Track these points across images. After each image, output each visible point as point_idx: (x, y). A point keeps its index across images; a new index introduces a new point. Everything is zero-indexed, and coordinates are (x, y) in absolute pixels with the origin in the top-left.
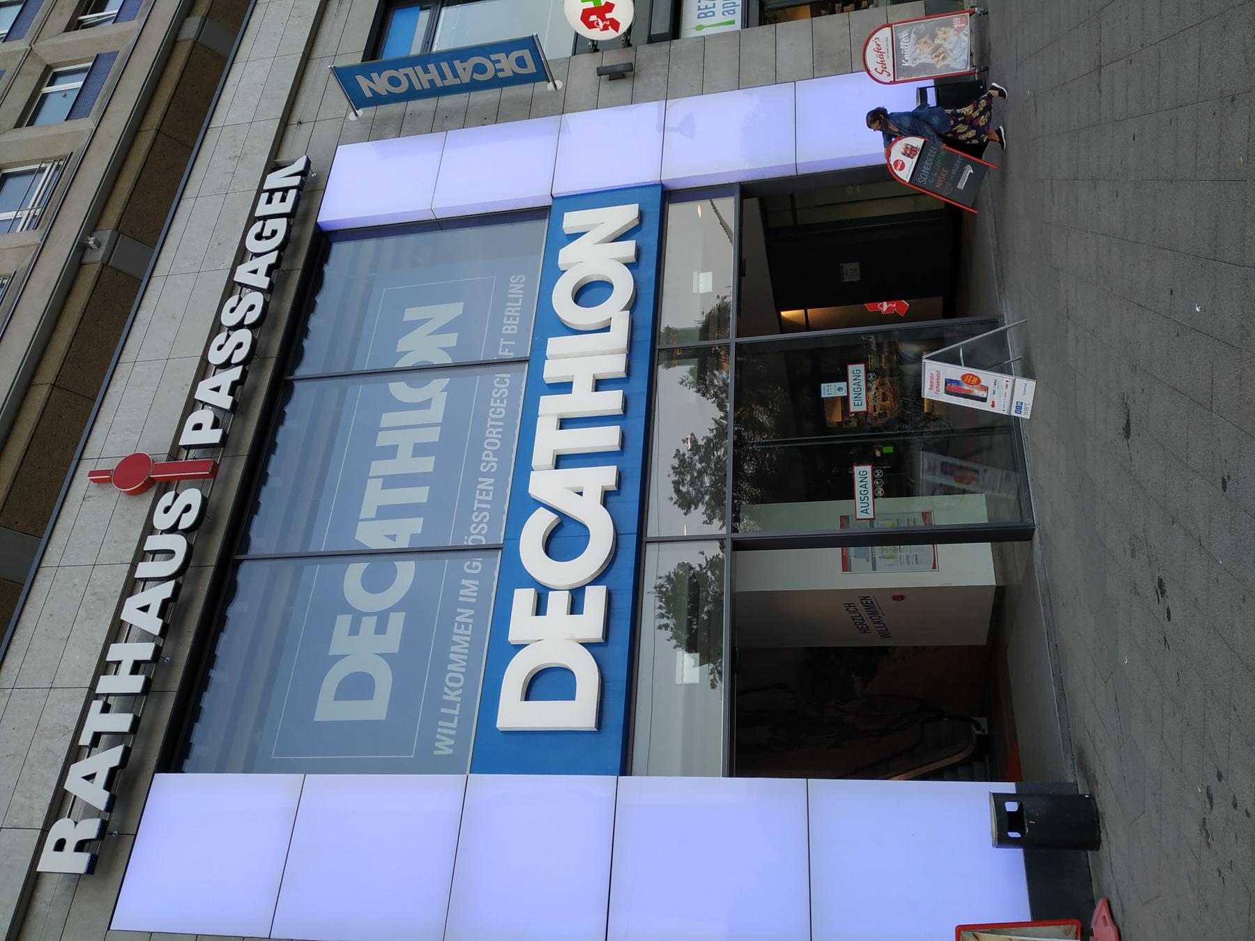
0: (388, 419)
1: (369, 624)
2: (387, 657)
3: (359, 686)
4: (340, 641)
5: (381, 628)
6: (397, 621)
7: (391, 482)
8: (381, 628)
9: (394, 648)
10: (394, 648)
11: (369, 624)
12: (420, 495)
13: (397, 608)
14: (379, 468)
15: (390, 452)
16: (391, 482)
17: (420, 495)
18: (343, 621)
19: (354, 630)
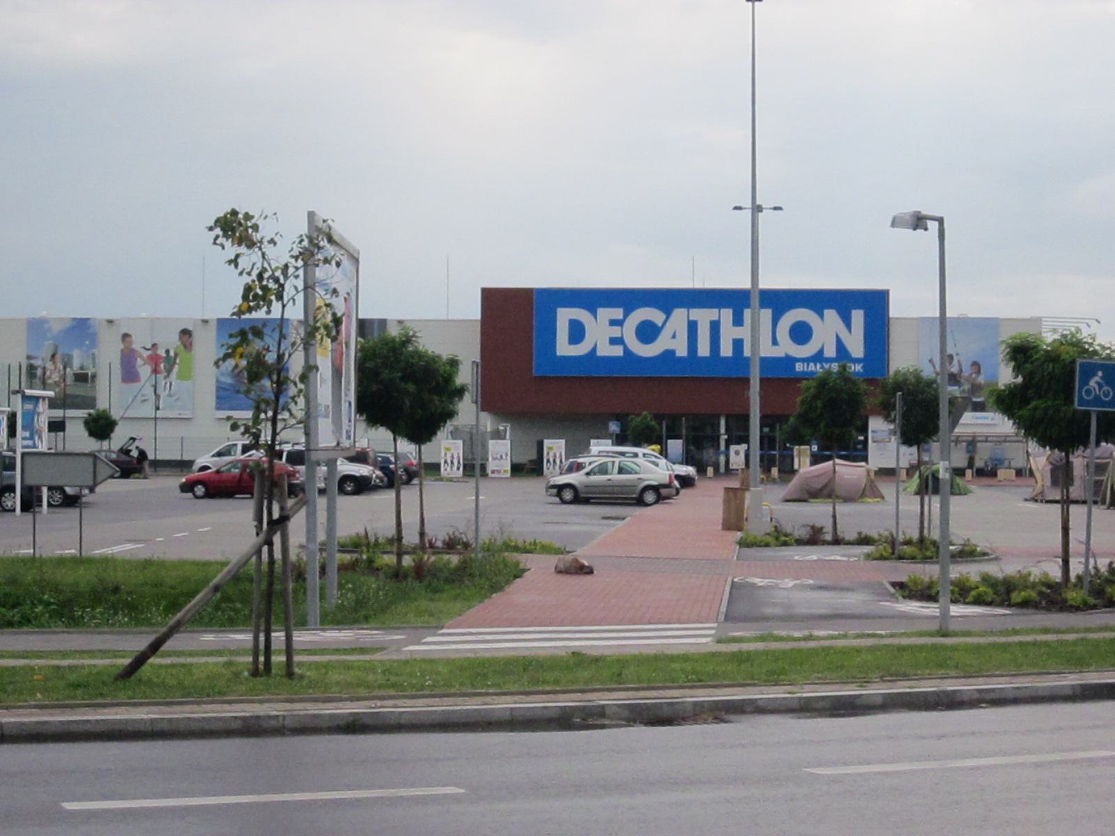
0: (766, 314)
1: (616, 332)
2: (594, 349)
3: (577, 333)
4: (606, 314)
5: (614, 341)
6: (618, 351)
7: (715, 327)
8: (614, 341)
9: (600, 353)
10: (600, 353)
11: (616, 332)
12: (704, 350)
13: (626, 350)
14: (727, 315)
15: (738, 321)
16: (715, 327)
17: (704, 350)
18: (618, 313)
19: (613, 323)
